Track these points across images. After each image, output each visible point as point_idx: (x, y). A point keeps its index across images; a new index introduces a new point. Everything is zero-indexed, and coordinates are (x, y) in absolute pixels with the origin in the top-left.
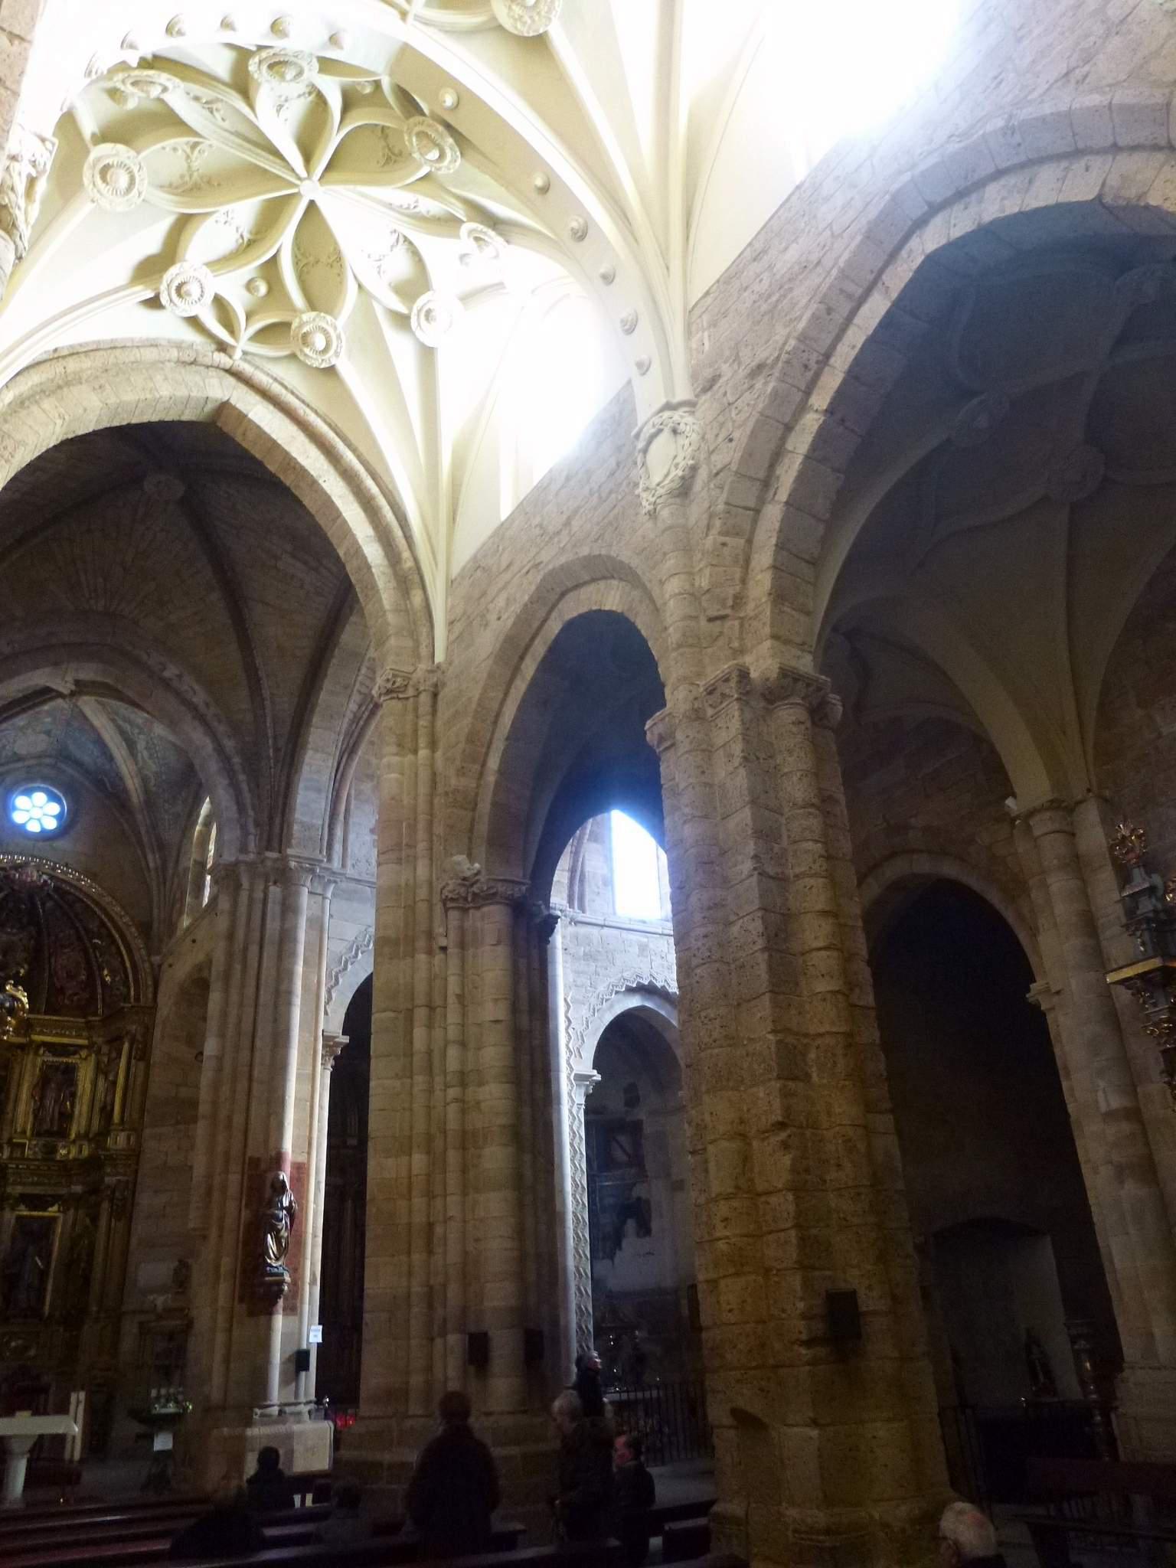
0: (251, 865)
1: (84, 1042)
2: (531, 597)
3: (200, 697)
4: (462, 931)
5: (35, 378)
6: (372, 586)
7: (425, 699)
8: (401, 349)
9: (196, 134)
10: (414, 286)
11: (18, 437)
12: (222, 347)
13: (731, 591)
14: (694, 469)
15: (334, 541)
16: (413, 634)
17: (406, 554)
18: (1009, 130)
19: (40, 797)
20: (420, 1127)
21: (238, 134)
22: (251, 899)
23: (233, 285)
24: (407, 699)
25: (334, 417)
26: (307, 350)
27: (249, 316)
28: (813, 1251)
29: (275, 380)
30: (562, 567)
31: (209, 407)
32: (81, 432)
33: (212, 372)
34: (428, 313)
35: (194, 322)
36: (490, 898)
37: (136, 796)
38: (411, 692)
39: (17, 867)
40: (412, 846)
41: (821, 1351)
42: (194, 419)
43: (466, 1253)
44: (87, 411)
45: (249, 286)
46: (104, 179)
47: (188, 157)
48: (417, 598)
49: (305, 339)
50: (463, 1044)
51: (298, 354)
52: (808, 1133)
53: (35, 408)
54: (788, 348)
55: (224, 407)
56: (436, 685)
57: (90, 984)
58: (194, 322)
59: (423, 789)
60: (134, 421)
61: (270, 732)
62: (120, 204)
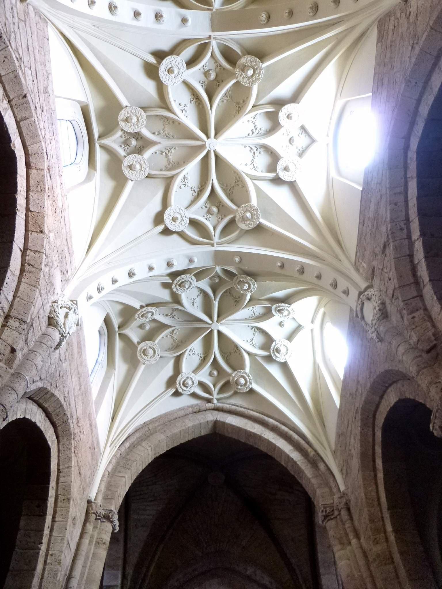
2: (361, 426)
6: (302, 472)
7: (344, 513)
8: (274, 371)
11: (133, 459)
12: (209, 401)
13: (430, 334)
14: (383, 303)
15: (278, 460)
16: (327, 485)
17: (310, 450)
18: (408, 82)
21: (185, 321)
23: (204, 376)
24: (336, 517)
25: (261, 410)
26: (239, 387)
29: (233, 405)
30: (365, 401)
31: (210, 425)
32: (161, 453)
33: (208, 412)
35: (194, 395)
38: (336, 513)
42: (207, 433)
45: (211, 374)
46: (145, 355)
47: (172, 337)
48: (322, 466)
49: (237, 383)
51: (236, 390)
53: (139, 447)
54: (389, 229)
55: (216, 423)
56: (346, 504)
58: (194, 395)
59: (361, 562)
60: (182, 442)
62: (153, 361)
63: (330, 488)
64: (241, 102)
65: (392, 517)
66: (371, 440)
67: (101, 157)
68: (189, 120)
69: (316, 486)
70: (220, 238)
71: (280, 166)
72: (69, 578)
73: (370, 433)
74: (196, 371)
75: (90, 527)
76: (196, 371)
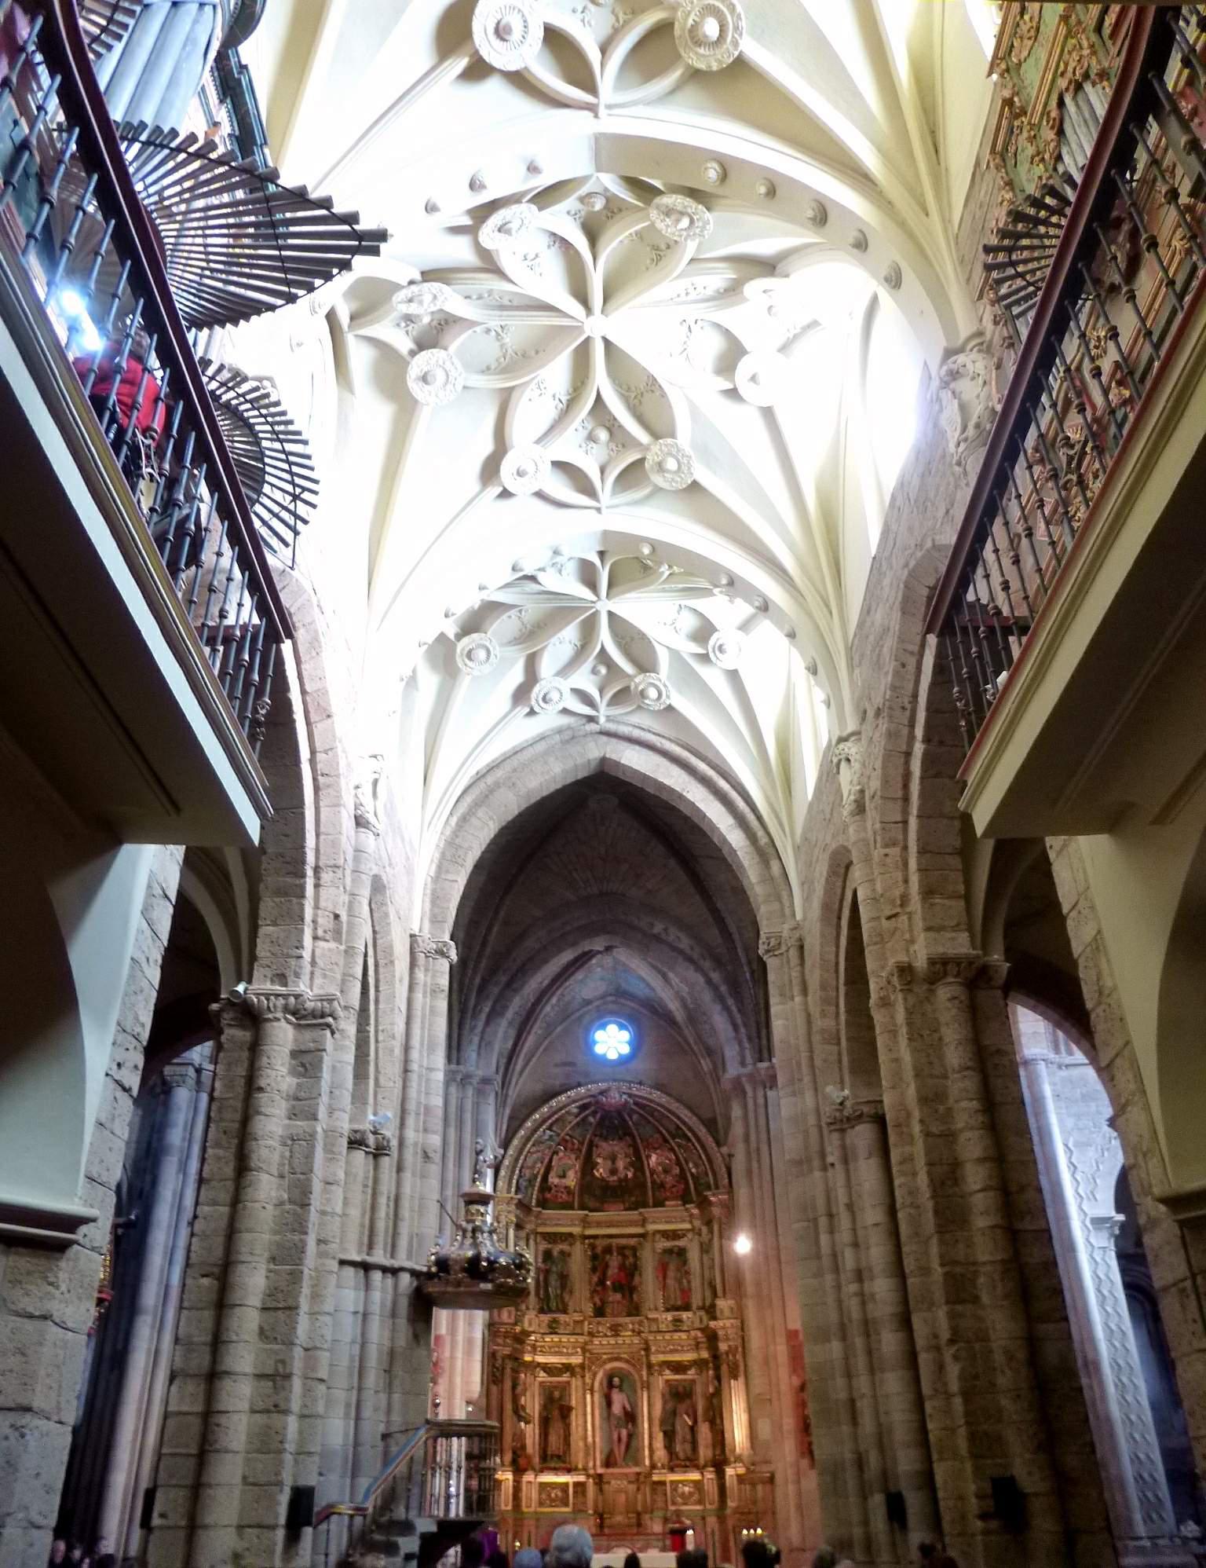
0: (751, 1077)
1: (688, 1226)
3: (685, 943)
4: (843, 1147)
5: (469, 799)
7: (793, 953)
8: (713, 677)
9: (513, 606)
10: (704, 632)
11: (466, 845)
12: (591, 719)
13: (897, 893)
14: (862, 791)
16: (779, 899)
17: (760, 833)
19: (612, 1028)
20: (834, 1317)
22: (755, 1104)
23: (584, 679)
27: (601, 691)
28: (984, 1444)
31: (593, 765)
32: (510, 818)
33: (589, 739)
34: (720, 647)
36: (859, 1118)
37: (679, 1016)
38: (784, 948)
39: (602, 1093)
40: (800, 1080)
41: (994, 1524)
43: (880, 1425)
44: (510, 805)
45: (594, 671)
46: (470, 659)
49: (643, 694)
50: (856, 1245)
52: (977, 1346)
55: (604, 760)
56: (800, 939)
57: (682, 1176)
59: (802, 1030)
61: (744, 960)
62: (486, 669)
63: (782, 909)
64: (663, 247)
65: (847, 994)
66: (839, 891)
67: (360, 357)
68: (552, 287)
69: (760, 899)
70: (614, 492)
71: (744, 368)
72: (407, 1048)
73: (839, 884)
74: (565, 671)
75: (420, 975)
76: (565, 671)
